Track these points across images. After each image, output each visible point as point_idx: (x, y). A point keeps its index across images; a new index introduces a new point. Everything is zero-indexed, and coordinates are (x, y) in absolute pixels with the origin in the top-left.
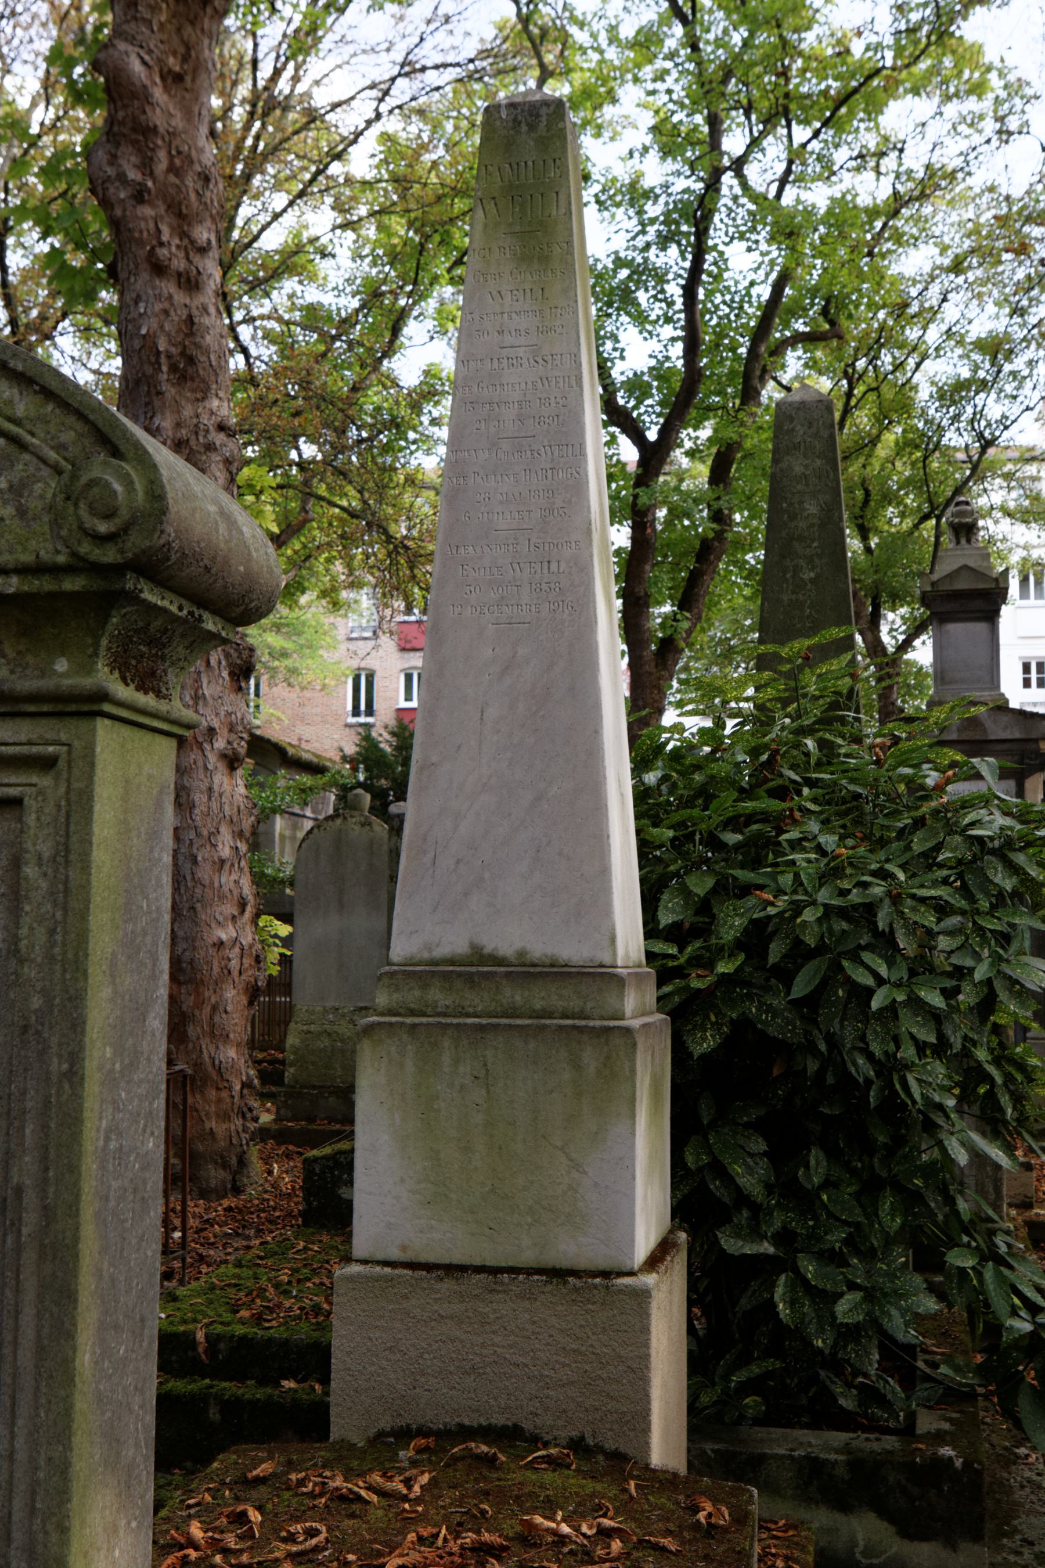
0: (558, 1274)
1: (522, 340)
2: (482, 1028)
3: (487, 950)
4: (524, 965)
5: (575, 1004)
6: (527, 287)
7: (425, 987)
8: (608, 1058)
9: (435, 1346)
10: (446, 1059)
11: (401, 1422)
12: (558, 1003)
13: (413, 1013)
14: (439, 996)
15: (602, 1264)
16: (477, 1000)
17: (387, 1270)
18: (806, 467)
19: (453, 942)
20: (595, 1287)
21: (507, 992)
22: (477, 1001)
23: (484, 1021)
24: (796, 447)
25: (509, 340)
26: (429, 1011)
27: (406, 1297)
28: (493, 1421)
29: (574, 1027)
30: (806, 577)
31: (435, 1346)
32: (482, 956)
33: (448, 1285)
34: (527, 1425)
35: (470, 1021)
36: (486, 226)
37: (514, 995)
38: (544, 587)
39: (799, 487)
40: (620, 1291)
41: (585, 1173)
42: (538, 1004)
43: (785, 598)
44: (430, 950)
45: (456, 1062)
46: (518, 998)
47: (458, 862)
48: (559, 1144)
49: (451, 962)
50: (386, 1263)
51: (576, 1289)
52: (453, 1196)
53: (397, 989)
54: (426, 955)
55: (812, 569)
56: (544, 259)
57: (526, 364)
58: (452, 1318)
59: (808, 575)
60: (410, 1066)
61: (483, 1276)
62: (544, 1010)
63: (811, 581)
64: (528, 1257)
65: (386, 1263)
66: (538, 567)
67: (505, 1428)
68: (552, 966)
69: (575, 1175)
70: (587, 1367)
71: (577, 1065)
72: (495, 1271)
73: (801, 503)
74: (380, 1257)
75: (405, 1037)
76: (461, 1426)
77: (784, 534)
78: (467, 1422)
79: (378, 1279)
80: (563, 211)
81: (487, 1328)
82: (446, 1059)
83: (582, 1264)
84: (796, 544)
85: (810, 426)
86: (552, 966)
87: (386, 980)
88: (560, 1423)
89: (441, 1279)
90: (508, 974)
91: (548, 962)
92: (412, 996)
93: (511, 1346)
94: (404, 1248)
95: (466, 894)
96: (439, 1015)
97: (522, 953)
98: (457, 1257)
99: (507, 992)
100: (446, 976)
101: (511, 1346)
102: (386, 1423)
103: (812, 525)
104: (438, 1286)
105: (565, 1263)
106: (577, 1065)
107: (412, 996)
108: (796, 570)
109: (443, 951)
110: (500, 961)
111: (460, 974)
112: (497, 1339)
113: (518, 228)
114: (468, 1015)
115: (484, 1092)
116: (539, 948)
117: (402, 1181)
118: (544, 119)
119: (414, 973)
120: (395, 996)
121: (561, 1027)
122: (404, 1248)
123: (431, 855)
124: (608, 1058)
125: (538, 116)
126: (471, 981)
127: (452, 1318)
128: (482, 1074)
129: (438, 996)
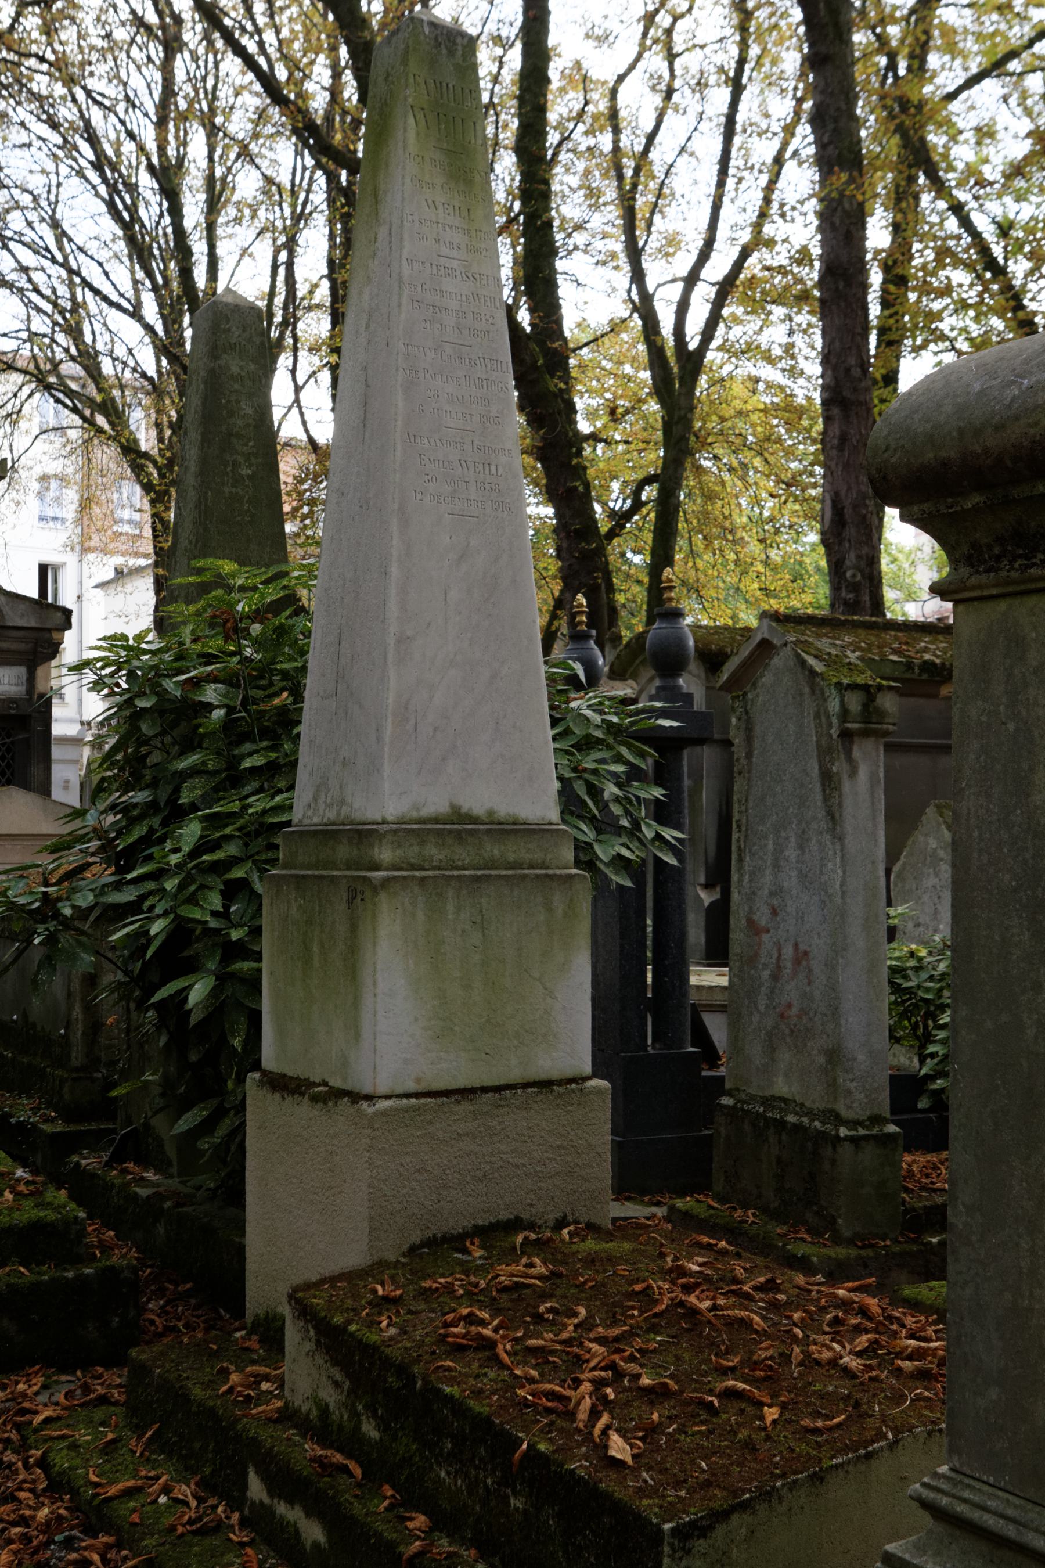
0: (545, 1085)
1: (454, 253)
2: (478, 879)
3: (464, 810)
4: (492, 823)
5: (538, 856)
6: (457, 205)
7: (423, 843)
8: (571, 900)
9: (455, 1162)
10: (450, 908)
11: (428, 1234)
12: (526, 857)
13: (413, 867)
14: (434, 851)
15: (569, 1073)
16: (464, 854)
17: (413, 1101)
18: (241, 368)
19: (436, 804)
20: (573, 1091)
21: (488, 846)
22: (464, 855)
23: (480, 873)
24: (232, 347)
25: (445, 251)
26: (427, 865)
27: (430, 1123)
28: (501, 1217)
29: (547, 875)
30: (244, 472)
31: (455, 1162)
32: (460, 815)
33: (465, 1107)
34: (525, 1216)
35: (466, 872)
36: (418, 134)
37: (493, 850)
38: (487, 486)
39: (236, 386)
40: (591, 1092)
41: (556, 998)
42: (511, 857)
43: (226, 490)
44: (418, 810)
45: (458, 909)
46: (496, 852)
47: (436, 729)
48: (537, 975)
49: (436, 820)
50: (408, 1096)
51: (559, 1095)
52: (457, 1028)
53: (399, 846)
54: (415, 814)
55: (250, 466)
56: (469, 182)
57: (459, 277)
58: (467, 1135)
59: (246, 472)
60: (420, 915)
61: (490, 1095)
62: (515, 862)
63: (248, 476)
64: (515, 1075)
65: (408, 1096)
66: (481, 467)
67: (509, 1221)
68: (514, 824)
69: (549, 1000)
70: (569, 1159)
71: (549, 909)
72: (498, 1089)
73: (238, 402)
74: (400, 1090)
75: (416, 889)
76: (476, 1226)
77: (224, 428)
78: (480, 1223)
79: (407, 1110)
80: (480, 142)
81: (495, 1139)
82: (450, 908)
83: (555, 1075)
84: (234, 440)
85: (244, 331)
86: (514, 824)
87: (389, 837)
88: (549, 1208)
89: (458, 1102)
90: (489, 831)
91: (511, 820)
92: (412, 852)
93: (513, 1151)
94: (418, 1080)
95: (444, 759)
96: (434, 868)
97: (491, 813)
98: (462, 1082)
99: (488, 846)
100: (439, 833)
101: (513, 1151)
102: (416, 1238)
103: (248, 425)
104: (456, 1108)
105: (543, 1077)
106: (549, 909)
107: (412, 852)
108: (236, 465)
109: (427, 811)
110: (475, 820)
111: (450, 832)
112: (503, 1147)
113: (445, 146)
114: (457, 868)
115: (480, 935)
116: (504, 808)
117: (416, 1019)
118: (460, 48)
119: (413, 830)
120: (398, 852)
121: (537, 876)
122: (418, 1080)
123: (412, 722)
124: (571, 900)
125: (455, 44)
126: (459, 836)
127: (467, 1135)
128: (478, 919)
129: (434, 852)
